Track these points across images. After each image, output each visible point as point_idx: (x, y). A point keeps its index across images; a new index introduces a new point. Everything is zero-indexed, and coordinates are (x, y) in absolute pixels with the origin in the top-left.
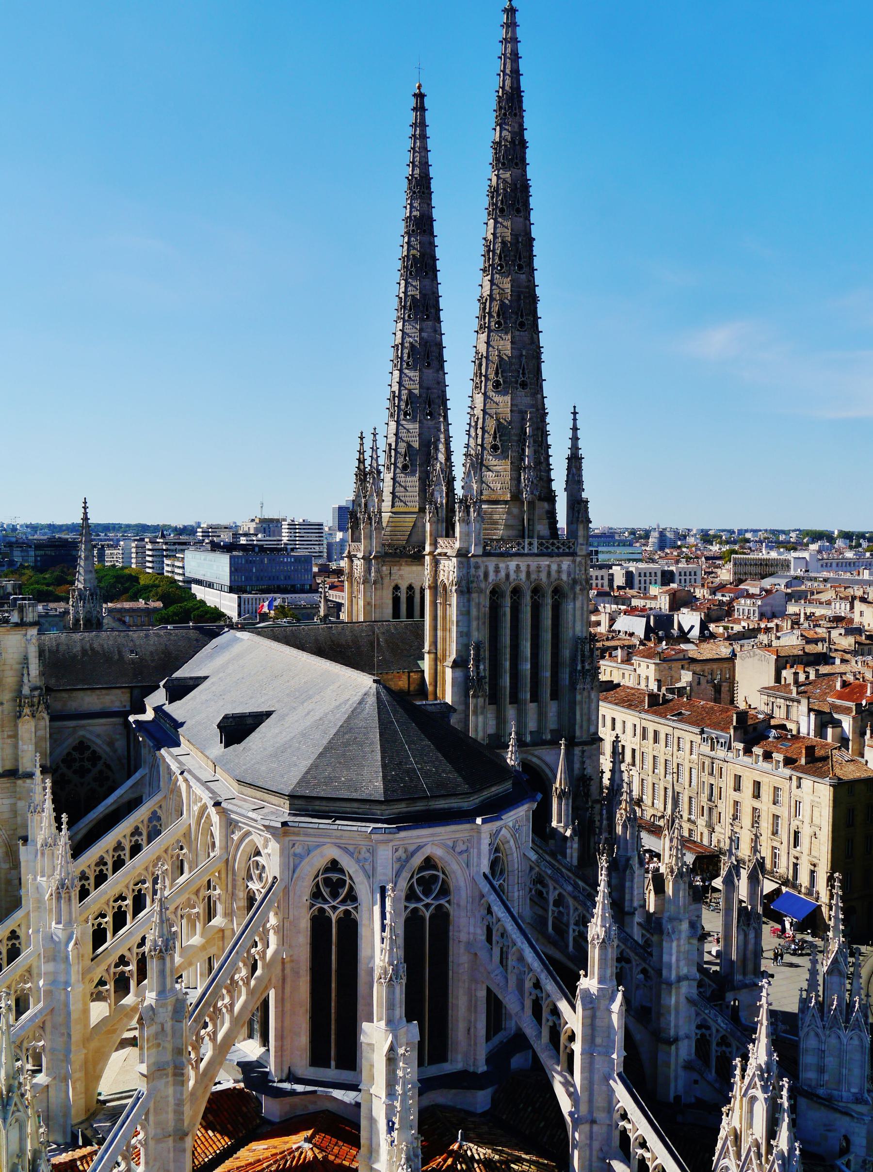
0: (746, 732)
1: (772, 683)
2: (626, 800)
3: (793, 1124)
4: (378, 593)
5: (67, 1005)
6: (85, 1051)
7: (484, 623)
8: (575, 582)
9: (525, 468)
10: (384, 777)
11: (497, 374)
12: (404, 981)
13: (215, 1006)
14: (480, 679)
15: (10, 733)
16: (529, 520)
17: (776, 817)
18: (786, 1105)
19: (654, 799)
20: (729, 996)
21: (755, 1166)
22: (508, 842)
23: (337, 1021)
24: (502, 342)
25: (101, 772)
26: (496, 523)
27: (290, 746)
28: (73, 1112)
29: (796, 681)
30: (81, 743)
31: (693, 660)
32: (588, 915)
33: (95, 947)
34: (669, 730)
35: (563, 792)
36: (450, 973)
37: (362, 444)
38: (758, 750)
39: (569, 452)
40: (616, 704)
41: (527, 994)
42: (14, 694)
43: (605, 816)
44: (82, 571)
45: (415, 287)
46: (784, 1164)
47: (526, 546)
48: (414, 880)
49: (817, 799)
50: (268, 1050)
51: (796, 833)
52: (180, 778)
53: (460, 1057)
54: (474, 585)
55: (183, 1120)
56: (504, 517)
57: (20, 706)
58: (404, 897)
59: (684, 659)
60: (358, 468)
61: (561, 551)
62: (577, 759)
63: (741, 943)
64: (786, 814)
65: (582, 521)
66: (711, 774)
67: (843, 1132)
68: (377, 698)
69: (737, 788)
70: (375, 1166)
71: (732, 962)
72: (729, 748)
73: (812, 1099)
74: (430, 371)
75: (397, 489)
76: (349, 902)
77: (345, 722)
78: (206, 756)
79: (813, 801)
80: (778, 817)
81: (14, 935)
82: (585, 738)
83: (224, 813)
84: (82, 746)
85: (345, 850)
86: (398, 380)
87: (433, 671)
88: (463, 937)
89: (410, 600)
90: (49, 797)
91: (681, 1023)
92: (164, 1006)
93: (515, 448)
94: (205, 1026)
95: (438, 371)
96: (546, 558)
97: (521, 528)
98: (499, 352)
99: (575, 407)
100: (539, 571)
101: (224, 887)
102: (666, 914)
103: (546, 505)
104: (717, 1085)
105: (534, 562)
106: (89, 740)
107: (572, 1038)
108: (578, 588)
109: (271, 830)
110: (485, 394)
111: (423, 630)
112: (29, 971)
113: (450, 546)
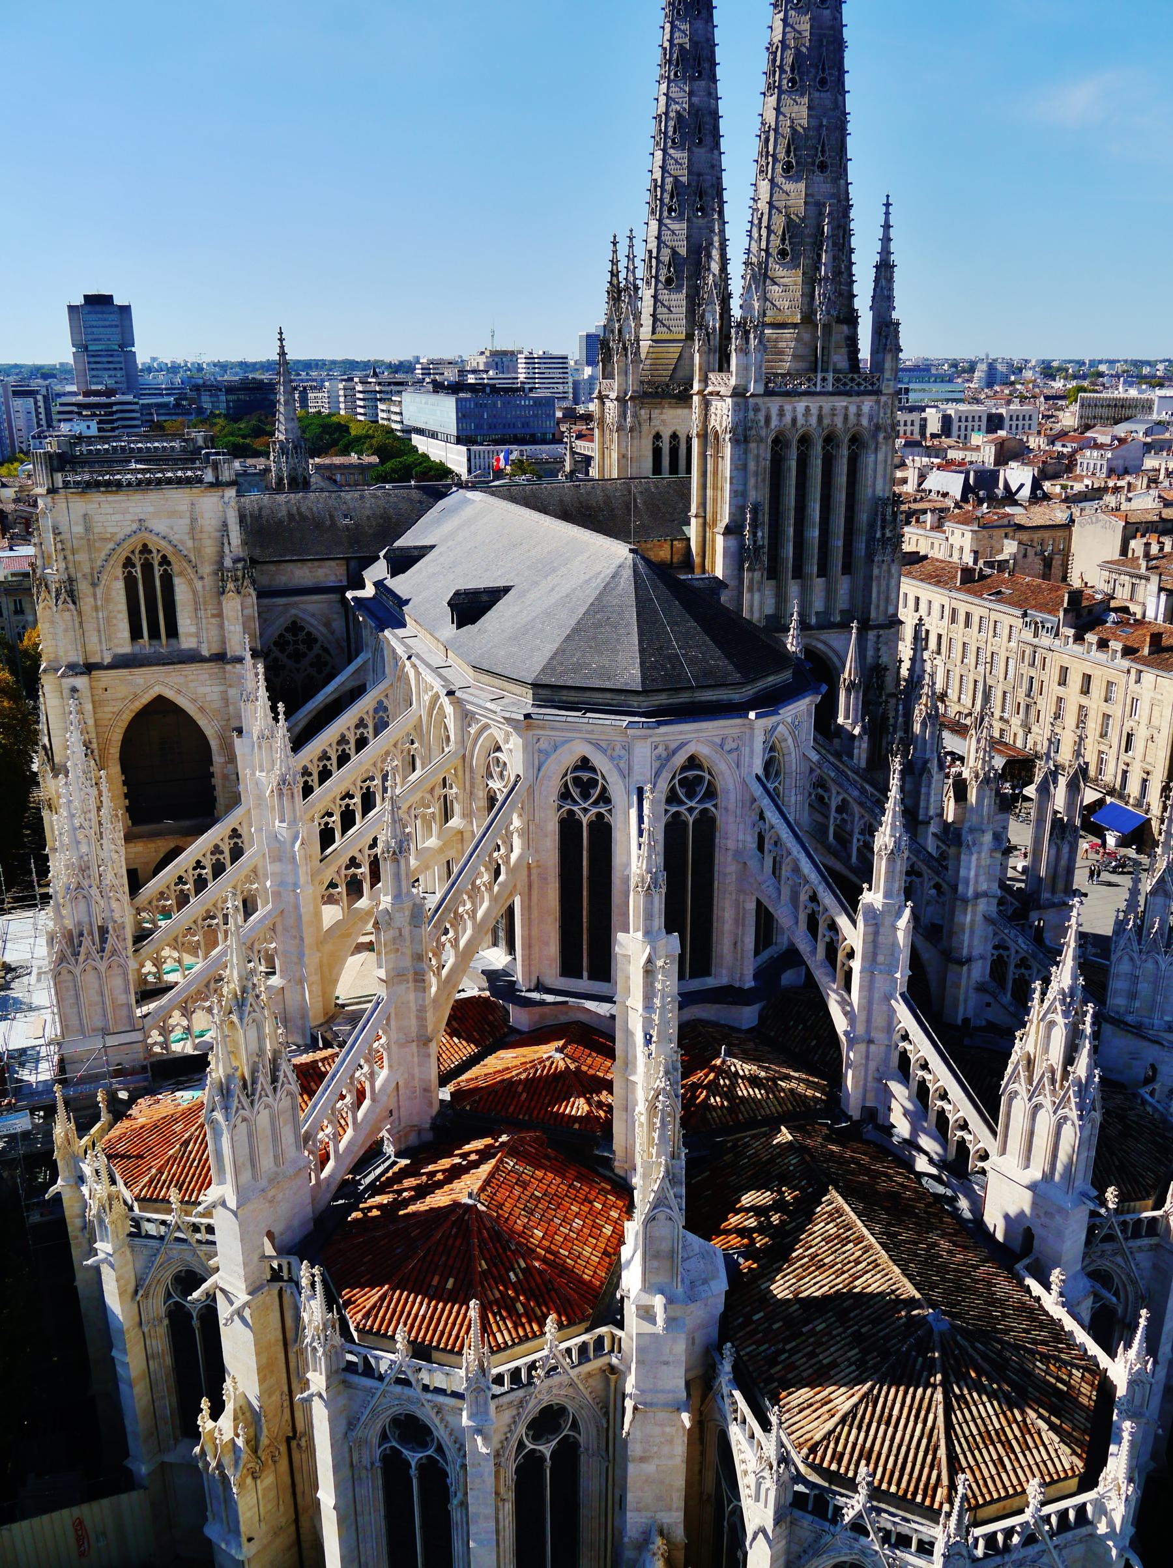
0: (1078, 616)
1: (1116, 555)
2: (927, 694)
3: (1095, 1050)
4: (636, 442)
5: (297, 907)
7: (764, 480)
8: (878, 428)
9: (820, 280)
10: (642, 664)
11: (788, 152)
12: (664, 891)
13: (456, 912)
14: (757, 549)
15: (215, 612)
16: (823, 348)
17: (1107, 717)
18: (1088, 1031)
20: (1034, 915)
21: (1047, 1092)
22: (786, 740)
23: (589, 930)
24: (796, 108)
25: (318, 656)
26: (782, 353)
27: (533, 628)
28: (311, 1014)
29: (1147, 554)
30: (294, 623)
31: (1020, 527)
32: (875, 824)
33: (324, 847)
34: (984, 613)
35: (852, 683)
36: (716, 883)
37: (615, 252)
38: (1091, 637)
39: (878, 258)
40: (922, 580)
42: (216, 567)
44: (282, 419)
45: (683, 32)
46: (1080, 1091)
47: (819, 382)
48: (676, 781)
49: (1159, 697)
50: (515, 959)
51: (1129, 736)
52: (407, 663)
53: (724, 972)
54: (753, 432)
56: (792, 345)
57: (223, 580)
58: (664, 800)
59: (1009, 526)
60: (610, 283)
61: (862, 388)
63: (1052, 858)
64: (1119, 713)
65: (891, 350)
66: (1033, 665)
67: (1151, 1061)
69: (1063, 682)
70: (632, 1078)
71: (1040, 879)
72: (1057, 635)
73: (1118, 1026)
74: (702, 150)
75: (659, 310)
76: (601, 804)
77: (596, 599)
79: (1153, 699)
80: (1109, 716)
81: (235, 833)
82: (881, 620)
83: (458, 703)
84: (295, 627)
85: (597, 746)
86: (660, 163)
87: (700, 539)
88: (731, 844)
89: (674, 451)
90: (262, 684)
91: (976, 942)
92: (401, 910)
93: (808, 253)
94: (446, 932)
95: (712, 150)
96: (843, 398)
97: (813, 358)
98: (792, 122)
99: (888, 196)
100: (834, 415)
102: (967, 825)
103: (845, 328)
104: (1012, 1009)
105: (827, 403)
106: (302, 619)
107: (851, 955)
108: (881, 436)
110: (772, 181)
111: (689, 489)
112: (255, 871)
113: (723, 383)
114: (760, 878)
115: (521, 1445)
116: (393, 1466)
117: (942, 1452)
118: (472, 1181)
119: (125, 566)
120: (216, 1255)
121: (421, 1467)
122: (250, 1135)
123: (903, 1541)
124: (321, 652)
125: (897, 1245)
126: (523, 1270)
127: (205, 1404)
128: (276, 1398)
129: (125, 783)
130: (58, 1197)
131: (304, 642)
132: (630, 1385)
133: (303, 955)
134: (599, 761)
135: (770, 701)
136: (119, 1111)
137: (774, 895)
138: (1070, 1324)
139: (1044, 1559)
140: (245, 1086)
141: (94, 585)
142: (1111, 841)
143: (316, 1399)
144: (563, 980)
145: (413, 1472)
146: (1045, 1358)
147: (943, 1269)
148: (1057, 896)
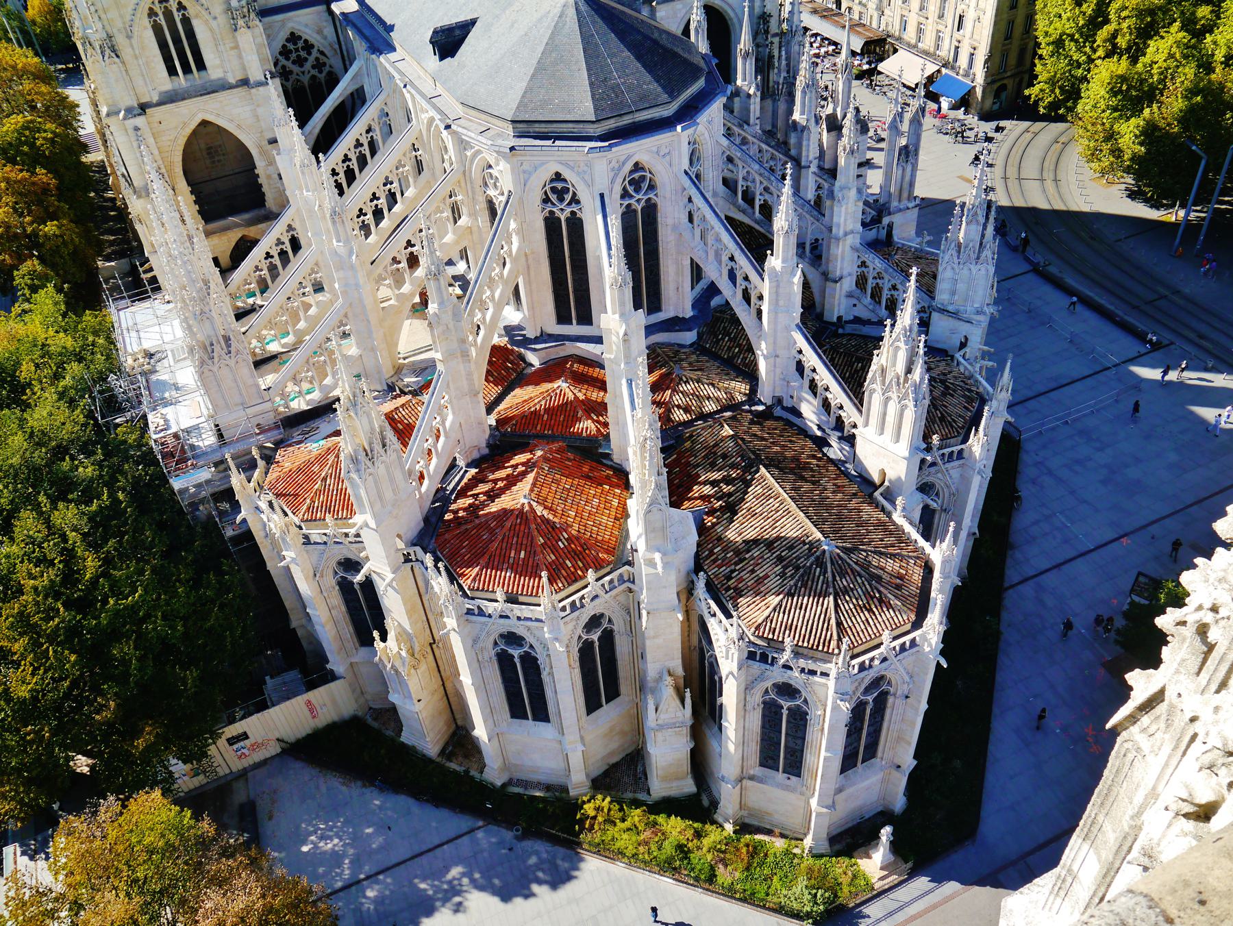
5: (361, 300)
10: (593, 96)
12: (631, 285)
13: (481, 300)
15: (232, 45)
18: (921, 352)
25: (317, 59)
28: (384, 370)
30: (292, 34)
35: (747, 54)
41: (724, 265)
43: (784, 57)
51: (961, 17)
52: (404, 90)
53: (671, 308)
63: (899, 177)
71: (890, 194)
77: (550, 38)
81: (290, 228)
84: (293, 38)
85: (566, 165)
88: (670, 221)
91: (846, 265)
104: (871, 307)
112: (316, 264)
115: (580, 637)
116: (504, 661)
117: (833, 622)
118: (525, 486)
119: (150, 16)
120: (364, 549)
121: (521, 657)
122: (376, 482)
123: (812, 673)
124: (319, 55)
125: (801, 496)
126: (566, 539)
127: (376, 634)
128: (419, 625)
129: (192, 192)
130: (244, 521)
131: (303, 49)
132: (644, 597)
134: (566, 174)
135: (688, 112)
136: (269, 459)
137: (704, 256)
138: (908, 528)
139: (892, 667)
140: (367, 455)
141: (129, 37)
142: (945, 103)
143: (452, 632)
145: (517, 660)
146: (893, 556)
147: (829, 507)
148: (902, 203)
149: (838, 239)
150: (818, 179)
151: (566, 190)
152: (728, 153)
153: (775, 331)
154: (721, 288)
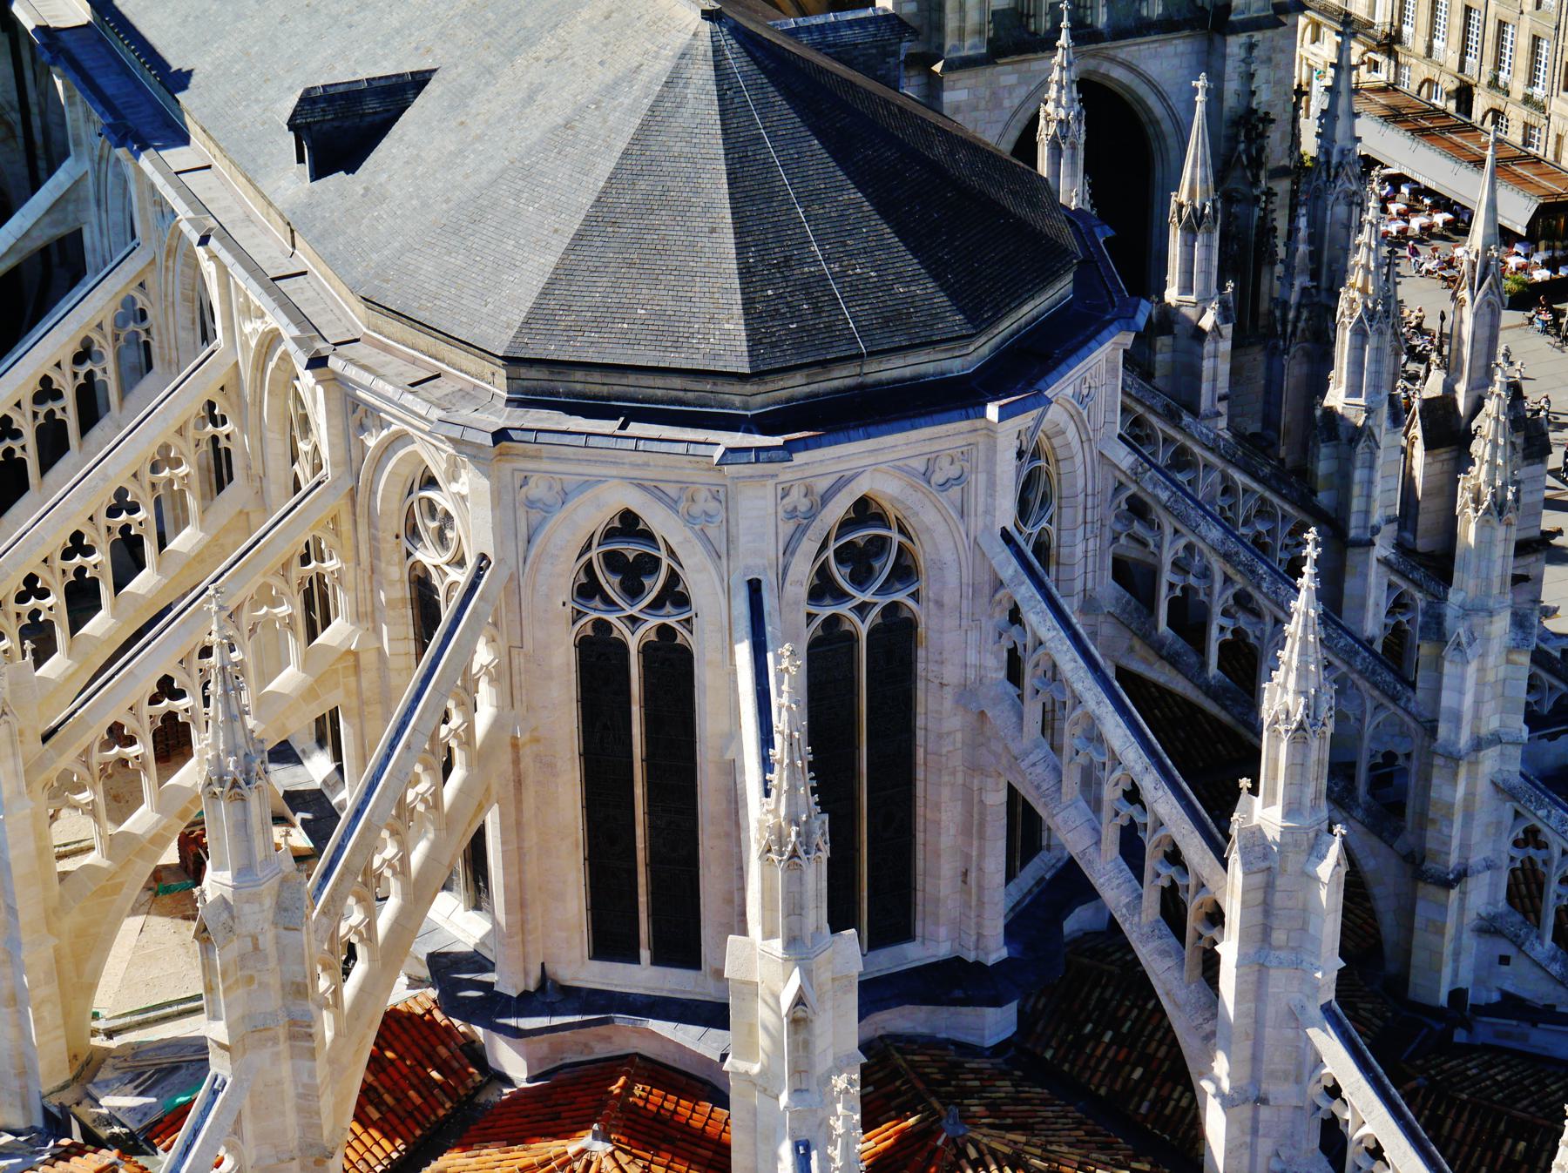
2: (1366, 268)
6: (53, 942)
10: (748, 304)
12: (825, 854)
13: (367, 869)
19: (1432, 36)
23: (652, 864)
28: (42, 1066)
43: (1303, 234)
52: (200, 251)
53: (943, 932)
55: (320, 1127)
58: (805, 595)
62: (1232, 69)
68: (717, 68)
76: (669, 608)
77: (635, 140)
78: (259, 192)
83: (337, 384)
85: (654, 490)
88: (951, 674)
91: (1476, 835)
92: (254, 898)
101: (351, 554)
109: (468, 450)
114: (1015, 748)
133: (19, 945)
134: (655, 518)
144: (598, 966)
149: (1454, 759)
150: (1394, 578)
151: (652, 564)
152: (1133, 489)
153: (1258, 1021)
154: (1098, 881)
